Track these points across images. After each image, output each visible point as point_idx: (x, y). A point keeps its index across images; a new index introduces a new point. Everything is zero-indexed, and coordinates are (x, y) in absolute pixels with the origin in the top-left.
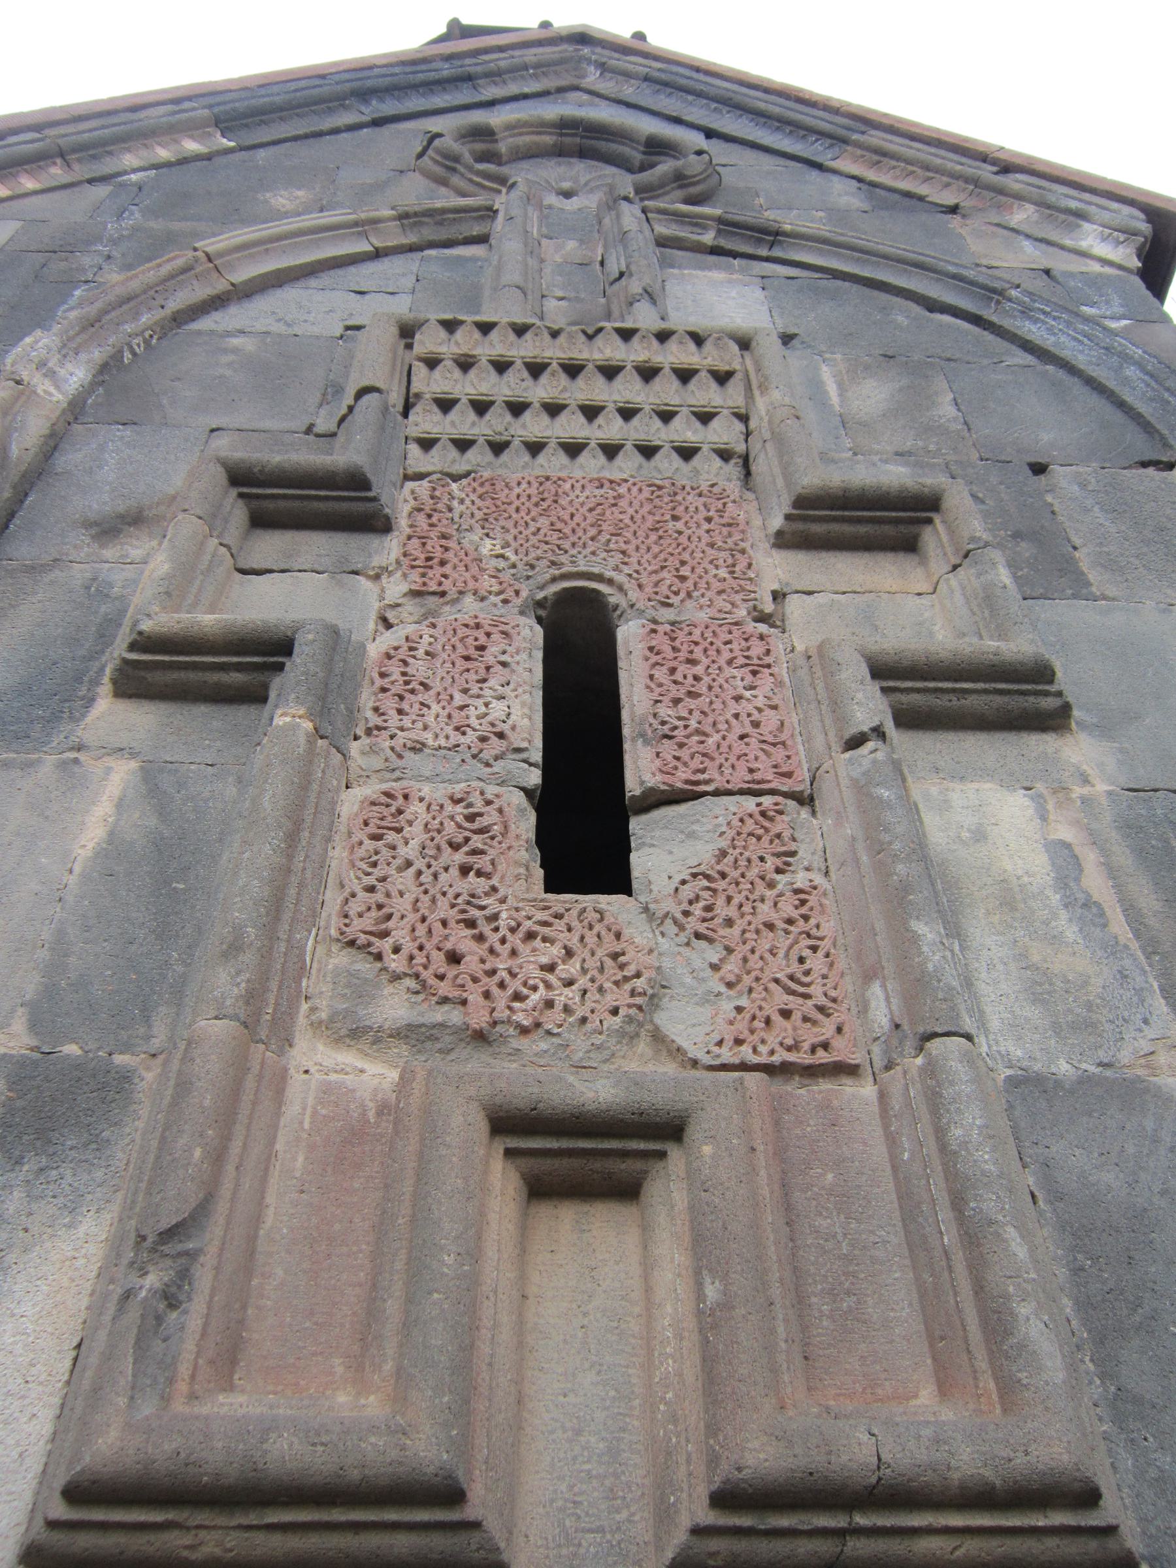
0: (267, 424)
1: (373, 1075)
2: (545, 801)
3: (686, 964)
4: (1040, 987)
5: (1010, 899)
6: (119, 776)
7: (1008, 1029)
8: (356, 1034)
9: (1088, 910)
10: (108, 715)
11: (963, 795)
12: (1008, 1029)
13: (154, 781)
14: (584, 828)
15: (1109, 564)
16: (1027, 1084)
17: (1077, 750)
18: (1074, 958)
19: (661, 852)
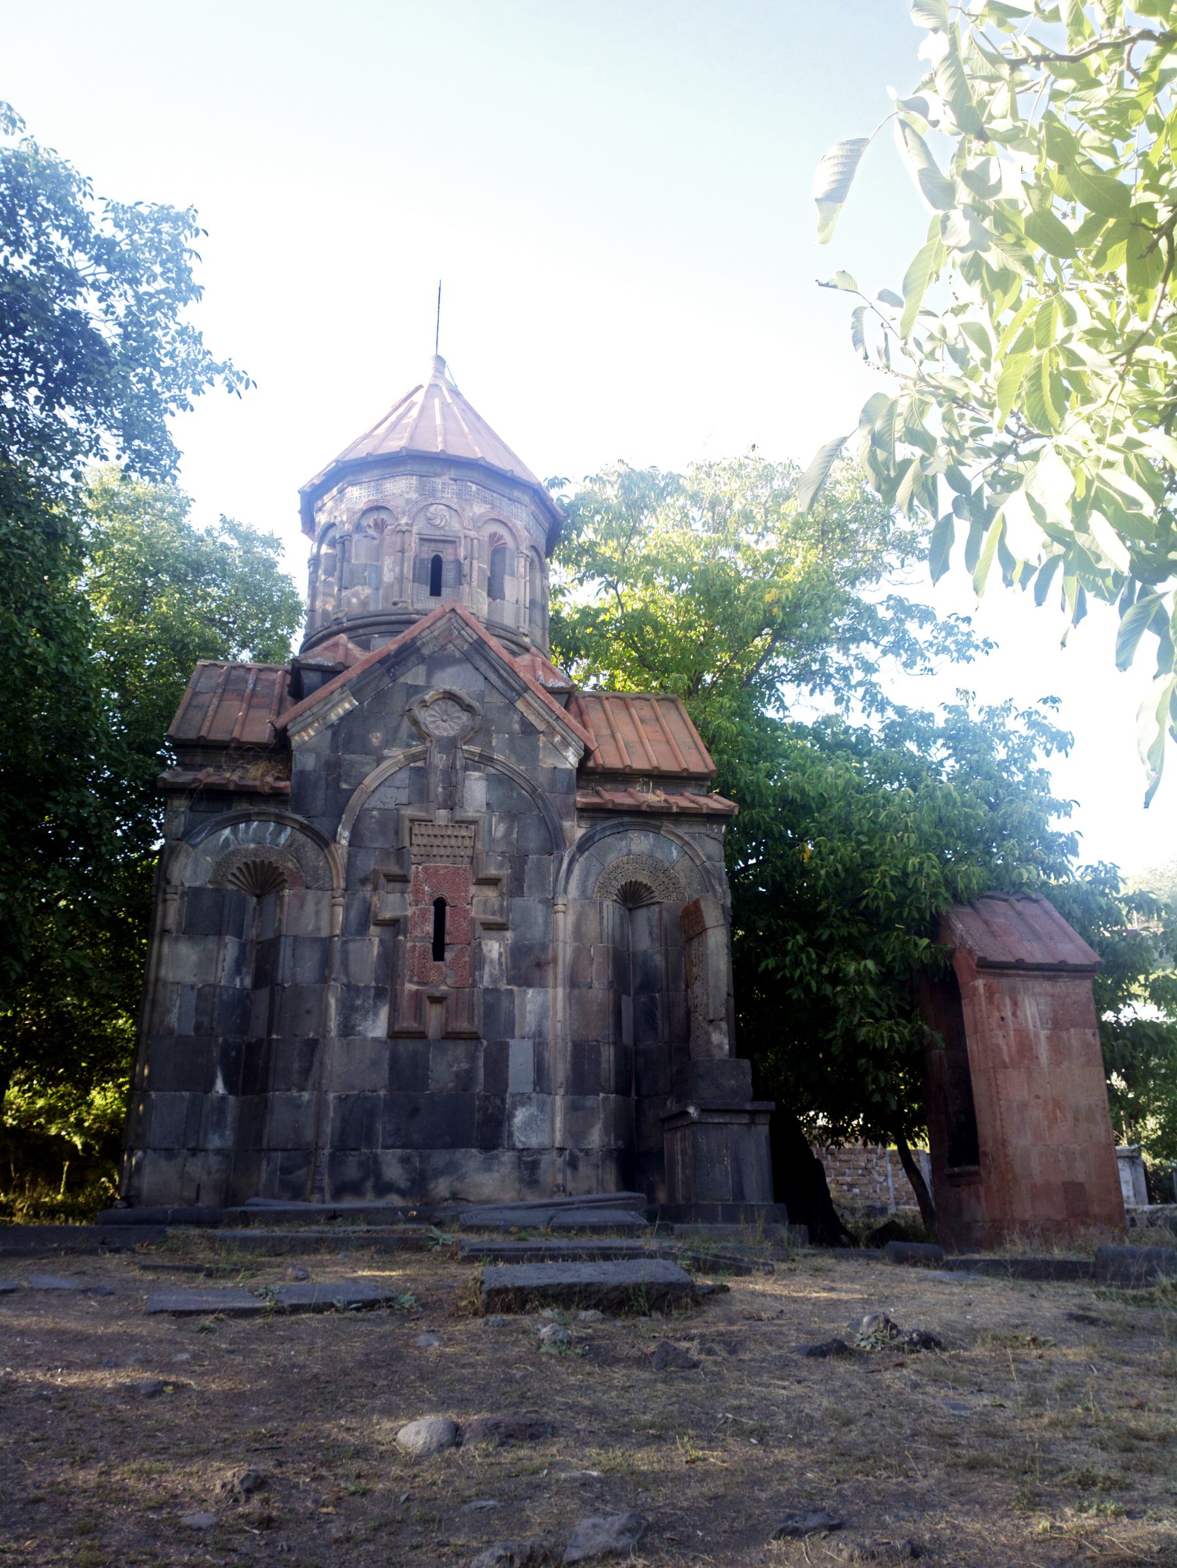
0: (386, 846)
1: (414, 987)
2: (434, 949)
3: (450, 972)
4: (491, 976)
5: (492, 961)
6: (376, 941)
7: (486, 982)
8: (411, 981)
9: (500, 964)
10: (373, 929)
11: (490, 943)
12: (486, 982)
13: (381, 941)
14: (439, 951)
15: (529, 888)
16: (486, 990)
17: (509, 934)
18: (497, 972)
19: (448, 955)
